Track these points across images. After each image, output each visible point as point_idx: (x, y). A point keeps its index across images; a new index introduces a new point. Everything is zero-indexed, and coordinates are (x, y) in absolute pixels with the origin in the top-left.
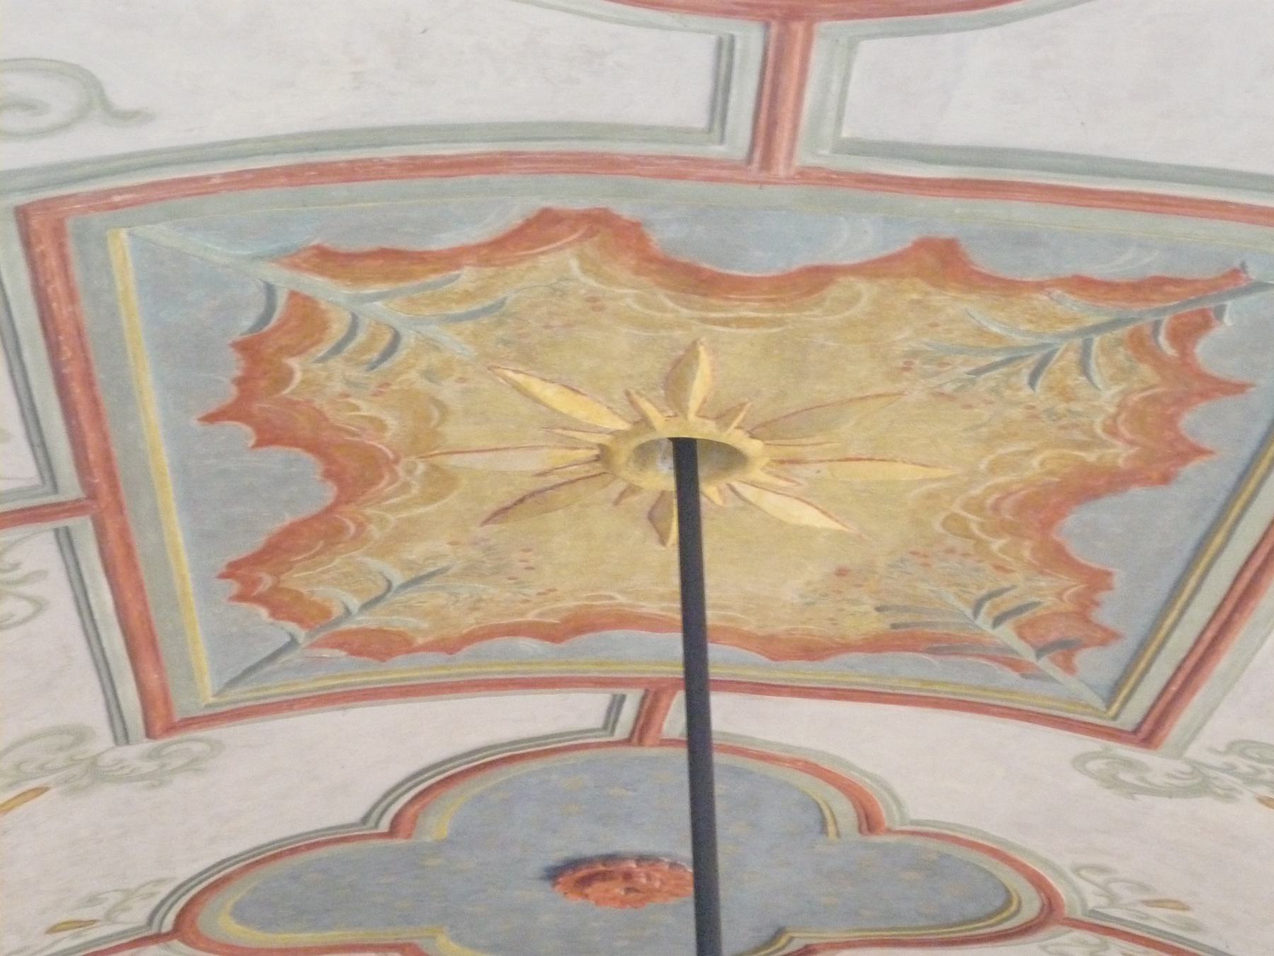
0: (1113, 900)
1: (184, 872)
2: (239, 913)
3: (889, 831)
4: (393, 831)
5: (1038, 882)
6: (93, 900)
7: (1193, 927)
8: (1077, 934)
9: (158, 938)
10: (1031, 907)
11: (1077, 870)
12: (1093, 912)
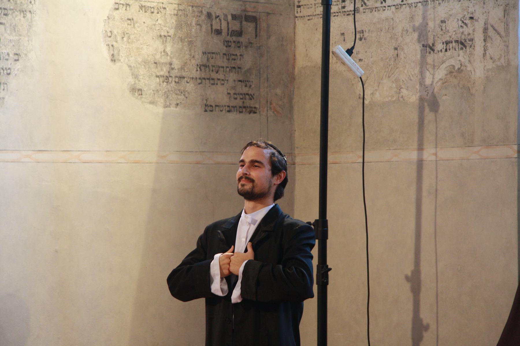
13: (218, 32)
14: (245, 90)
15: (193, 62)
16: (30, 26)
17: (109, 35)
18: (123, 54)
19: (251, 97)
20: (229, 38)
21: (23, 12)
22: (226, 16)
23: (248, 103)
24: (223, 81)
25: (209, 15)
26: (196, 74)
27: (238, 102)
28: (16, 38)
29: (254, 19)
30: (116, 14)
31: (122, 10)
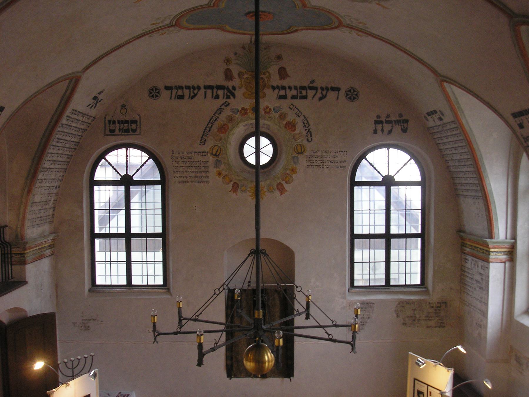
0: (352, 22)
1: (175, 14)
2: (187, 21)
3: (308, 7)
4: (214, 6)
5: (337, 18)
6: (158, 19)
7: (367, 28)
8: (346, 29)
9: (172, 26)
10: (337, 24)
11: (345, 16)
12: (348, 24)
13: (432, 307)
14: (441, 322)
15: (424, 315)
16: (373, 311)
17: (396, 311)
19: (443, 323)
20: (436, 308)
21: (371, 307)
22: (435, 303)
25: (429, 303)
29: (445, 303)
30: (399, 305)
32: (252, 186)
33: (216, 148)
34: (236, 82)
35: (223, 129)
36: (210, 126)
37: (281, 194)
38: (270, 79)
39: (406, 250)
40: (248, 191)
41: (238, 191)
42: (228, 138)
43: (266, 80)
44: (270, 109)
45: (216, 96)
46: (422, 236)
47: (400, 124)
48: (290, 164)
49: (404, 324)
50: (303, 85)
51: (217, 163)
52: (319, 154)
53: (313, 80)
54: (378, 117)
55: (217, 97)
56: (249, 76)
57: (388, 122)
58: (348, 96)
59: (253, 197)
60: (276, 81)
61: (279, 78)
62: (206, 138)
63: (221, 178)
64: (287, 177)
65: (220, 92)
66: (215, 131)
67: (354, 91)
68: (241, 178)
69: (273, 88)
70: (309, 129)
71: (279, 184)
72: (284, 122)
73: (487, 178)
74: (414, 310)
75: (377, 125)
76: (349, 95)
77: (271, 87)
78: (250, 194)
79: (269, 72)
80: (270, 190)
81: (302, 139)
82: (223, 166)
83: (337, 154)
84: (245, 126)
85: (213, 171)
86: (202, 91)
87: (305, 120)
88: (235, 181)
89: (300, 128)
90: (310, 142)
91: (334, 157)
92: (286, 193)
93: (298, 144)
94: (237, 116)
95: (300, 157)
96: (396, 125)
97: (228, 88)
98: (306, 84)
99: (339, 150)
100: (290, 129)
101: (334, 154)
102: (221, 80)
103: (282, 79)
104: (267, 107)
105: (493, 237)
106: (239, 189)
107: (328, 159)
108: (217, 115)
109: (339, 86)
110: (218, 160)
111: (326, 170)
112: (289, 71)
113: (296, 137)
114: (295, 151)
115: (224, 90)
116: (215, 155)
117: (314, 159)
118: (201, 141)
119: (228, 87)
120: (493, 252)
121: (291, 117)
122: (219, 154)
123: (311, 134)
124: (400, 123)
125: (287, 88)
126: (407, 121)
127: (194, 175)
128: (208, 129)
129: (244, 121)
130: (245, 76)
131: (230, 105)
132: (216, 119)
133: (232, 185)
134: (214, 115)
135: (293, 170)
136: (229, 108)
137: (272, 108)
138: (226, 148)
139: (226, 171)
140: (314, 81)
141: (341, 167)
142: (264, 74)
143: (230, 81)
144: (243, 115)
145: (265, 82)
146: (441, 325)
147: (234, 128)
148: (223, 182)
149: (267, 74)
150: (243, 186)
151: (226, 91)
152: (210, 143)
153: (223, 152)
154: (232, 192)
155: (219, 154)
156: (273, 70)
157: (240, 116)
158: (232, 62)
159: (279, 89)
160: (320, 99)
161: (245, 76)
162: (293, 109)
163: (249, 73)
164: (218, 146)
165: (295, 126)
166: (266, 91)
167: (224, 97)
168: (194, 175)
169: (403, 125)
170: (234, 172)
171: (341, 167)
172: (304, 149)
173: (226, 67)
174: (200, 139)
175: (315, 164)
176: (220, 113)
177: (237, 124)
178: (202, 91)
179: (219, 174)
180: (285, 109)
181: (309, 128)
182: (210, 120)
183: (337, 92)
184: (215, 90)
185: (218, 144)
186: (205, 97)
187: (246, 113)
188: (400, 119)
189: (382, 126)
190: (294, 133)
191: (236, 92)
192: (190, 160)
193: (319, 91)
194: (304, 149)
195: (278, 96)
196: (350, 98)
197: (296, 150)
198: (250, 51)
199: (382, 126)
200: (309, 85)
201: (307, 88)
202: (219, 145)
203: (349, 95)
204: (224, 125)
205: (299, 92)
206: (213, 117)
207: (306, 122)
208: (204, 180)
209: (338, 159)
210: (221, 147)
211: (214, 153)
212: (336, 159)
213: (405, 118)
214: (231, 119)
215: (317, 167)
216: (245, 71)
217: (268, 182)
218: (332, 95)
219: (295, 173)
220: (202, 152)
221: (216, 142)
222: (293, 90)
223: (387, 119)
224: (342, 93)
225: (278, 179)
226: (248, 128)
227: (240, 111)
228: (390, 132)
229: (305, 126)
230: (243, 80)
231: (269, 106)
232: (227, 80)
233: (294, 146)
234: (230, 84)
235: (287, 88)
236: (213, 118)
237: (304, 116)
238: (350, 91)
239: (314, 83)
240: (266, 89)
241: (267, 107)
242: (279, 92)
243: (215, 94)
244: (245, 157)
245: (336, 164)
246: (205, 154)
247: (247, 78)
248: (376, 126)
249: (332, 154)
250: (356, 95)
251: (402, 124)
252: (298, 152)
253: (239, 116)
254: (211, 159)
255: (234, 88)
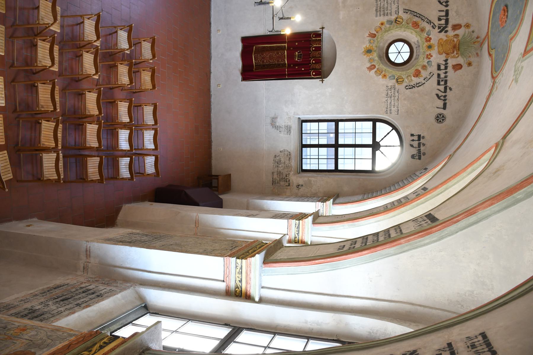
13: (286, 176)
14: (276, 182)
18: (281, 153)
19: (275, 184)
22: (289, 178)
23: (274, 183)
24: (278, 177)
25: (289, 174)
26: (279, 171)
27: (274, 181)
28: (283, 131)
29: (289, 185)
31: (289, 154)
32: (374, 47)
33: (401, 21)
34: (451, 33)
35: (416, 25)
36: (418, 16)
37: (368, 68)
38: (453, 58)
39: (327, 159)
40: (370, 45)
41: (370, 38)
42: (408, 28)
43: (453, 55)
44: (430, 58)
45: (440, 18)
46: (336, 170)
47: (418, 153)
48: (389, 74)
49: (276, 156)
50: (448, 82)
51: (390, 22)
52: (397, 94)
53: (452, 90)
54: (423, 137)
55: (440, 20)
56: (455, 42)
57: (419, 145)
58: (439, 116)
59: (365, 48)
60: (452, 62)
61: (453, 64)
62: (409, 13)
63: (380, 26)
64: (379, 72)
65: (443, 22)
66: (414, 19)
67: (443, 120)
68: (379, 40)
69: (446, 61)
70: (414, 87)
71: (375, 66)
72: (420, 69)
73: (376, 201)
74: (284, 163)
75: (417, 136)
76: (440, 116)
77: (446, 59)
78: (368, 46)
79: (458, 57)
80: (371, 60)
81: (408, 82)
82: (388, 26)
83: (396, 107)
84: (418, 41)
85: (384, 19)
86: (445, 9)
87: (422, 84)
88: (377, 35)
89: (415, 80)
90: (405, 88)
91: (394, 105)
92: (368, 72)
93: (403, 79)
94: (425, 34)
95: (394, 81)
96: (417, 150)
97: (446, 27)
98: (449, 84)
99: (399, 108)
100: (415, 73)
101: (396, 105)
102: (452, 22)
103: (453, 67)
104: (432, 56)
105: (334, 205)
106: (371, 38)
107: (392, 101)
108: (425, 21)
109: (447, 109)
110: (392, 22)
111: (385, 100)
112: (458, 72)
113: (409, 77)
114: (399, 77)
115: (444, 24)
116: (396, 20)
117: (393, 91)
118: (407, 10)
119: (447, 27)
120: (323, 204)
121: (424, 74)
122: (396, 23)
123: (411, 88)
124: (419, 154)
125: (446, 71)
126: (420, 159)
127: (382, 6)
128: (415, 14)
129: (421, 40)
130: (455, 40)
131: (434, 29)
132: (423, 20)
133: (374, 33)
134: (426, 18)
135: (385, 76)
136: (431, 29)
137: (431, 60)
138: (402, 28)
139: (384, 29)
140: (452, 90)
141: (387, 110)
142: (457, 54)
143: (452, 29)
144: (426, 39)
145: (450, 54)
146: (274, 182)
147: (416, 32)
148: (376, 27)
149: (457, 56)
150: (374, 41)
151: (444, 26)
152: (405, 16)
153: (398, 26)
154: (369, 33)
155: (396, 23)
156: (460, 60)
157: (425, 37)
158: (466, 29)
159: (445, 65)
160: (437, 95)
161: (455, 40)
162: (430, 75)
163: (458, 42)
164: (403, 22)
165: (417, 77)
166: (444, 55)
167: (439, 24)
168: (382, 6)
169: (417, 156)
170: (383, 34)
171: (387, 110)
172: (400, 84)
173: (463, 25)
174: (408, 9)
175: (389, 92)
176: (427, 22)
177: (419, 35)
178: (445, 9)
179: (382, 24)
180: (430, 69)
181: (416, 87)
182: (422, 15)
183: (442, 107)
184: (445, 18)
185: (404, 22)
186: (439, 11)
187: (427, 41)
188: (422, 154)
189: (416, 140)
190: (412, 76)
191: (443, 33)
192: (392, 3)
193: (444, 94)
194: (400, 84)
195: (440, 64)
196: (438, 117)
197: (399, 78)
198: (475, 42)
199: (416, 140)
200: (448, 86)
201: (445, 85)
202: (403, 23)
203: (440, 116)
204: (419, 26)
205: (442, 79)
206: (425, 17)
207: (420, 84)
208: (378, 13)
209: (392, 107)
210: (402, 24)
211: (397, 19)
212: (392, 106)
213: (422, 157)
214: (423, 30)
215: (387, 93)
216: (460, 39)
217: (377, 58)
218: (440, 103)
219: (383, 78)
220: (398, 11)
221: (405, 21)
222: (444, 75)
223: (421, 144)
224: (442, 111)
225: (379, 66)
226: (416, 45)
227: (429, 37)
228: (412, 146)
229: (417, 84)
230: (452, 38)
231: (433, 57)
232: (452, 26)
233: (402, 76)
234: (449, 28)
235: (446, 71)
236: (424, 18)
237: (425, 83)
238: (443, 117)
239: (449, 90)
240: (445, 55)
241: (432, 56)
242: (443, 64)
243: (442, 18)
244: (395, 44)
245: (389, 107)
246: (397, 12)
247: (454, 41)
248: (416, 135)
249: (396, 104)
250: (440, 121)
251: (418, 155)
252: (398, 79)
253: (425, 36)
254: (393, 17)
255: (446, 32)
